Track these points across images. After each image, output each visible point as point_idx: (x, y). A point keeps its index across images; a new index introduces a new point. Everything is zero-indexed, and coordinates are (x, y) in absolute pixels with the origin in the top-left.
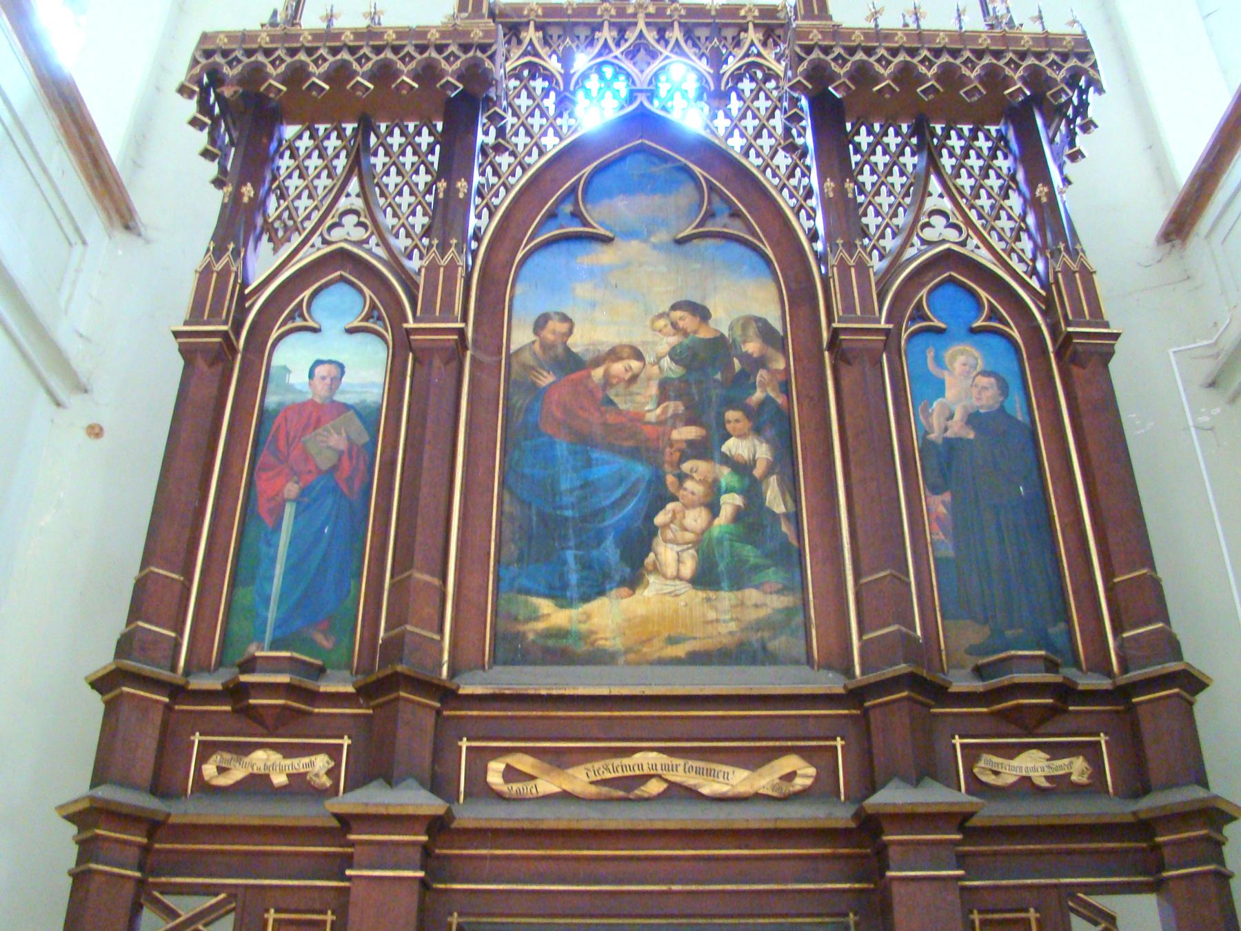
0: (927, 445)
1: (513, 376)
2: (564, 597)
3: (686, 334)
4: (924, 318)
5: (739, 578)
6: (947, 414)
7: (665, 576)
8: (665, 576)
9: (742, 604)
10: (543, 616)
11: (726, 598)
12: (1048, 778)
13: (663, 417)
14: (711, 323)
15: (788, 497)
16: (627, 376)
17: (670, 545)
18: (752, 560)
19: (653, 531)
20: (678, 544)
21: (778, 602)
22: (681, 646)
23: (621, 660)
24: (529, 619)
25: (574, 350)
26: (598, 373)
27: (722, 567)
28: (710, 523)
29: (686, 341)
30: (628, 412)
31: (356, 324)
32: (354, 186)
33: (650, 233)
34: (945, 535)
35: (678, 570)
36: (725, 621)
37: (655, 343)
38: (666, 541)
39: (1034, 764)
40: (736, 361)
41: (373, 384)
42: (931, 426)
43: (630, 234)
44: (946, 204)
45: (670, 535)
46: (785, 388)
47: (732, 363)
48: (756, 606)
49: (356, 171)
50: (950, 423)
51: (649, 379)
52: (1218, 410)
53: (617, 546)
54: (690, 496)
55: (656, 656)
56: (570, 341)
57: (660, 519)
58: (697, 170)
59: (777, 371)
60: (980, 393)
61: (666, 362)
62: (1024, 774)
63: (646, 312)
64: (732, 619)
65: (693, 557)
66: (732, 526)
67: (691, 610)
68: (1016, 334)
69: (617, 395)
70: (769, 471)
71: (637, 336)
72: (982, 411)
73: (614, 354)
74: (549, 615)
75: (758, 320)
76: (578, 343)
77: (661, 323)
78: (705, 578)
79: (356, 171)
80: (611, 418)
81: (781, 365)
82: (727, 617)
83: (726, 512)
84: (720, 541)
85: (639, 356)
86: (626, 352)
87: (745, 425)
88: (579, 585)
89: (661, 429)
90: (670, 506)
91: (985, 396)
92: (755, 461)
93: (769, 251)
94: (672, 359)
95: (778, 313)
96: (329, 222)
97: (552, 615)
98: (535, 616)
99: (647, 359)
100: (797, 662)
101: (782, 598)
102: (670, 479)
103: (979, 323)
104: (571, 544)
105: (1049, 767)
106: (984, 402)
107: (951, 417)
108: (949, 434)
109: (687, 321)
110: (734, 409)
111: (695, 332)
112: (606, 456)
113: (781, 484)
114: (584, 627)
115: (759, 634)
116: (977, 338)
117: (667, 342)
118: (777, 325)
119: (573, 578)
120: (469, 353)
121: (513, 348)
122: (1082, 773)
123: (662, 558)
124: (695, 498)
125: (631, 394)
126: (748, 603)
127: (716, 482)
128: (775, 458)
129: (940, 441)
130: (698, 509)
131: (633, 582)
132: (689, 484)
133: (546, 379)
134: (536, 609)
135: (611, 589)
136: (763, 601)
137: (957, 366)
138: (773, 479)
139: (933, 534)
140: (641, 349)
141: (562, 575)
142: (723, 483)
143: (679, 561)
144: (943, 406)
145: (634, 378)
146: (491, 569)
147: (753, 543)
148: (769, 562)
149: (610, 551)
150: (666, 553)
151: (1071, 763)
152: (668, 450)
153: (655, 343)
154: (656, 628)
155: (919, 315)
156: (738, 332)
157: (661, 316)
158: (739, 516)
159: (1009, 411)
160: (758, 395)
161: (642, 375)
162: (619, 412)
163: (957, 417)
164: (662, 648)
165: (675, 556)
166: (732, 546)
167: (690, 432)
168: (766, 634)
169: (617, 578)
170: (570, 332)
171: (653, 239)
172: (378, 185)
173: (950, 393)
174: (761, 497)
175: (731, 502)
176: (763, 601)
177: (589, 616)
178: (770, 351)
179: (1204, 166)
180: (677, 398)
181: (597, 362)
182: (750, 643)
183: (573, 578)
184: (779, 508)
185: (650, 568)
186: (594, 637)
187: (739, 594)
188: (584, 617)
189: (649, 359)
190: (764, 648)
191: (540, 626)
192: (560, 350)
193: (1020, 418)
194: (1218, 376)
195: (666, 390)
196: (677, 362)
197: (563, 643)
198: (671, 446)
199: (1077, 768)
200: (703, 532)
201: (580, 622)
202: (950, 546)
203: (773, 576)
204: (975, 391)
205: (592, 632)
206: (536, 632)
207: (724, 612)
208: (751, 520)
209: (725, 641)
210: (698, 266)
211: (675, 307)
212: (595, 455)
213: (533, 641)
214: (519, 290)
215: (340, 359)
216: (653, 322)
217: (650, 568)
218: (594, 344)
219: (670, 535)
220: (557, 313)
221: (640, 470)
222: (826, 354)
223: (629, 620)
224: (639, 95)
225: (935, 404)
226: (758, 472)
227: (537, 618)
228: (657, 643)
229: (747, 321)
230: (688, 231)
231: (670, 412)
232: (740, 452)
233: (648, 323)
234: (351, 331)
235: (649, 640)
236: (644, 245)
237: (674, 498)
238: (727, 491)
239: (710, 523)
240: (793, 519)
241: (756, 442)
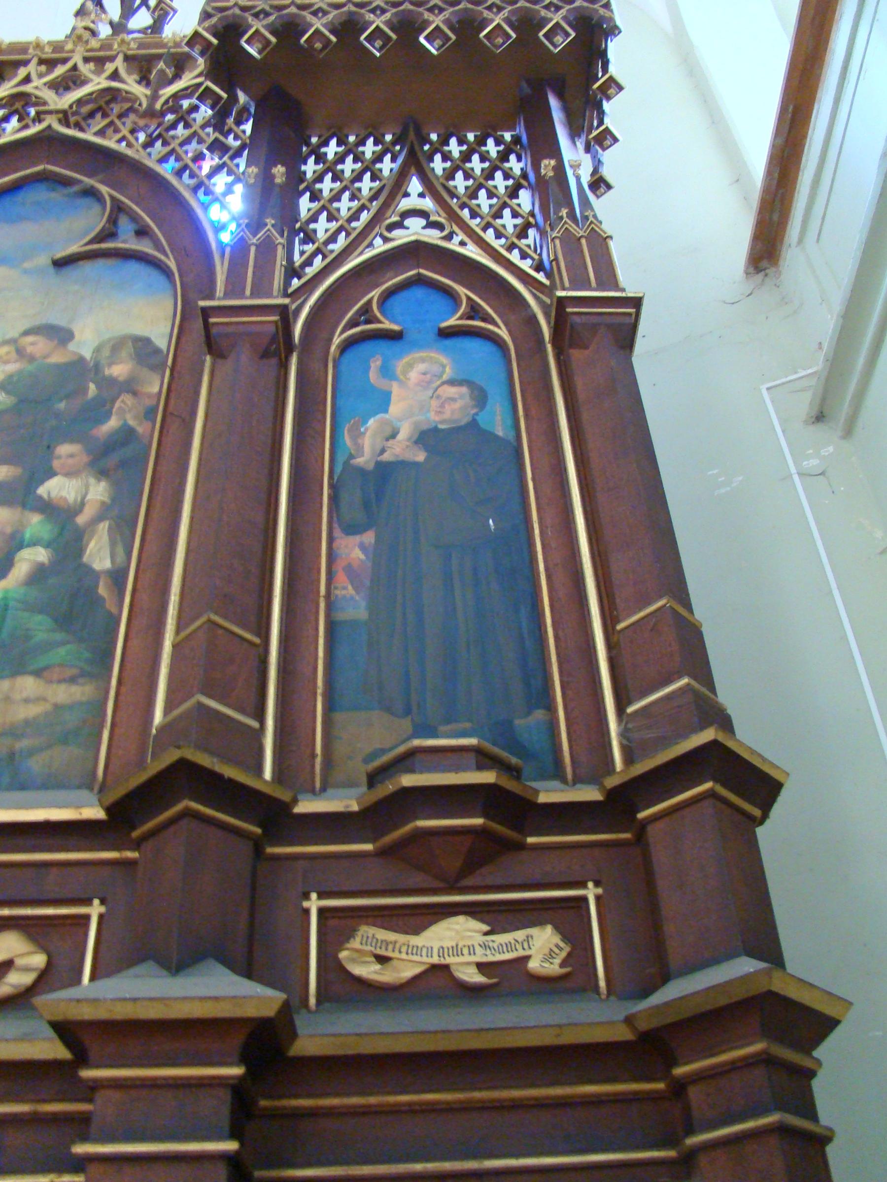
3: (32, 359)
6: (388, 431)
12: (482, 967)
14: (72, 346)
29: (30, 368)
34: (356, 588)
39: (459, 942)
40: (92, 387)
42: (360, 449)
47: (86, 390)
50: (391, 442)
52: (831, 449)
60: (442, 406)
62: (435, 960)
68: (503, 333)
72: (441, 426)
91: (453, 407)
92: (83, 504)
105: (485, 946)
106: (447, 415)
107: (393, 435)
108: (387, 457)
110: (72, 441)
116: (449, 342)
122: (551, 955)
128: (114, 500)
129: (371, 466)
137: (414, 375)
144: (387, 422)
151: (529, 937)
159: (482, 424)
163: (402, 436)
173: (395, 409)
179: (780, 141)
193: (500, 433)
194: (823, 400)
199: (541, 947)
202: (363, 604)
204: (434, 403)
225: (371, 422)
232: (64, 494)
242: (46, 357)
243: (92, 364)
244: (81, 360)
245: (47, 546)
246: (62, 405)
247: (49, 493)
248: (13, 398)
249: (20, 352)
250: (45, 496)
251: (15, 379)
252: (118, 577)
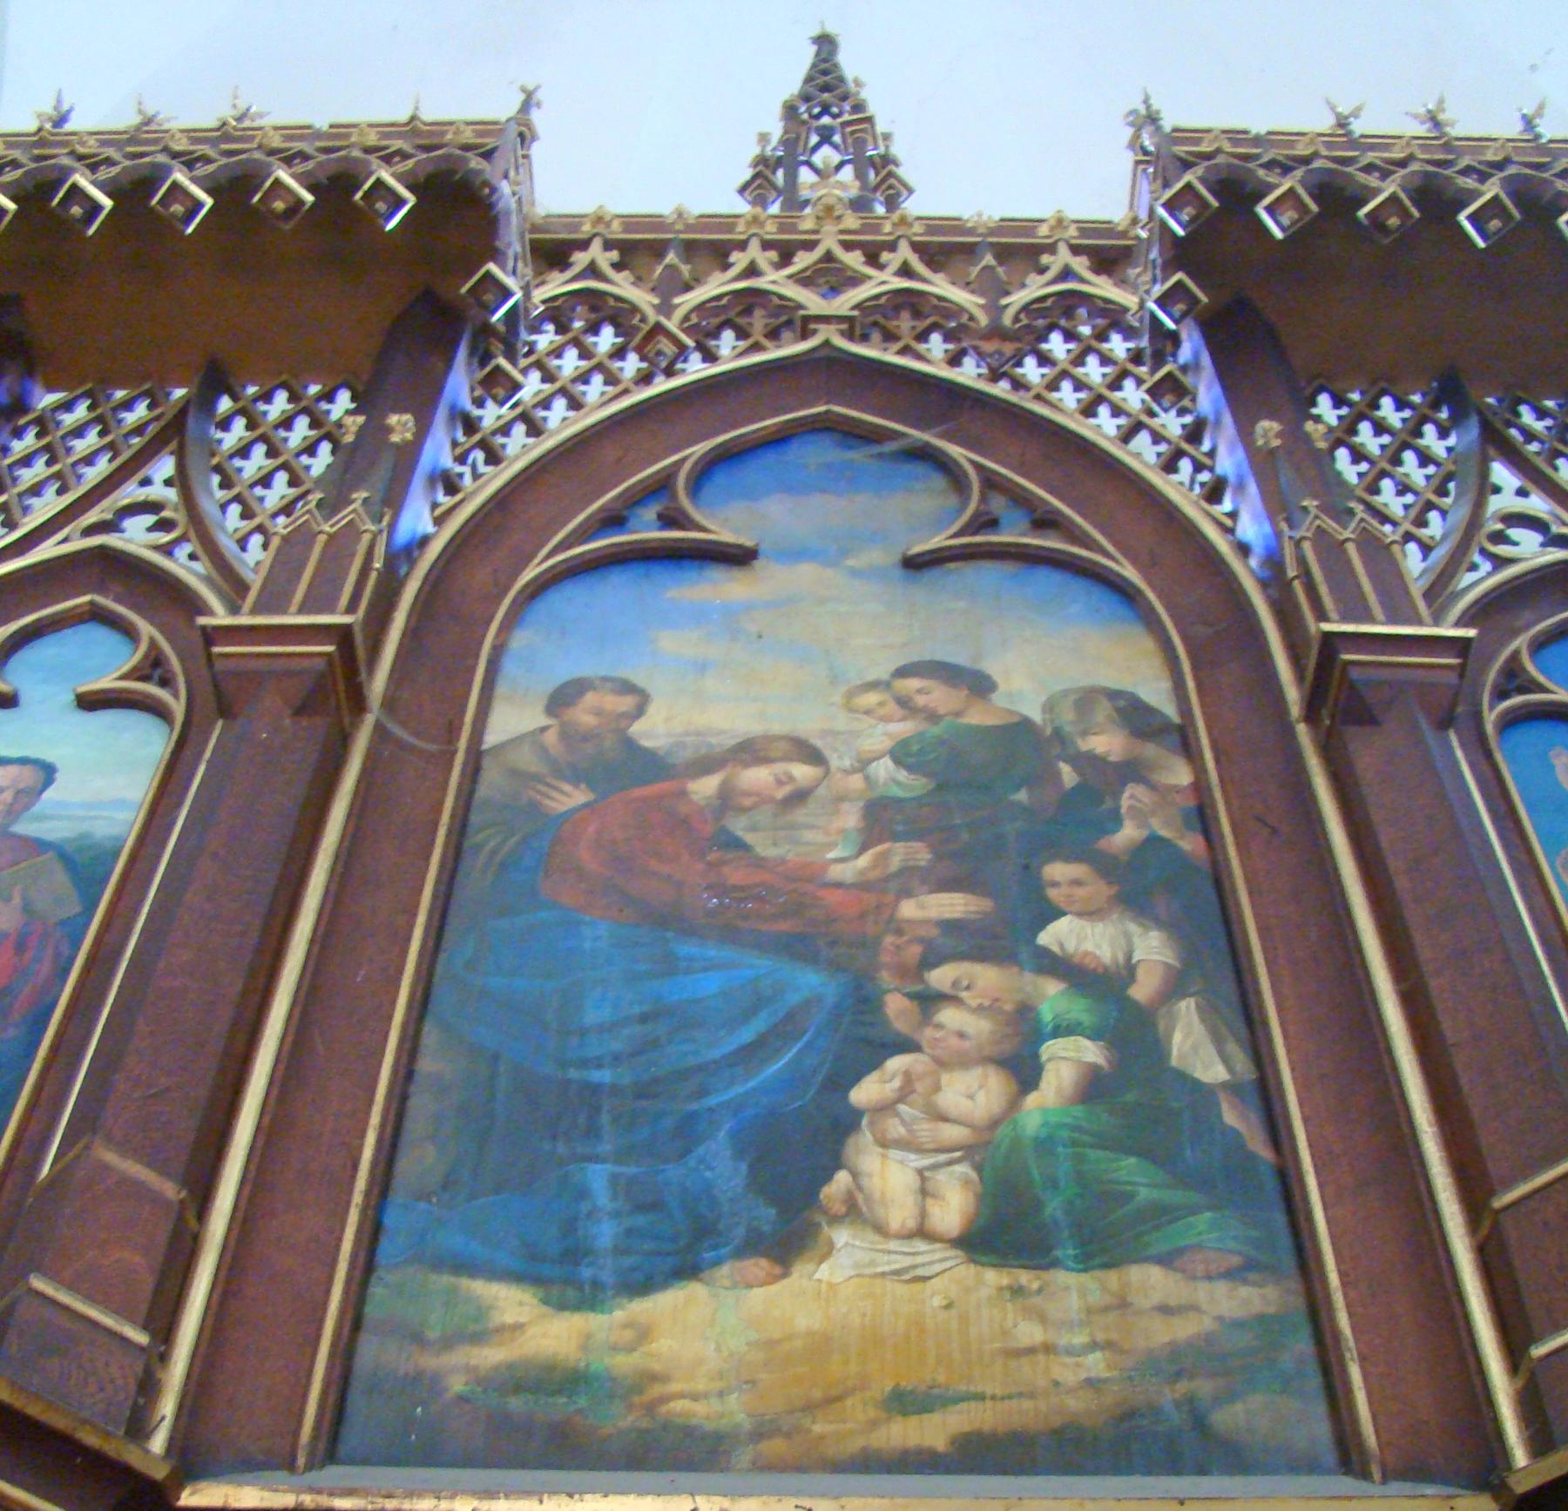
1: (482, 791)
2: (572, 1281)
3: (933, 717)
5: (1105, 1239)
7: (880, 1229)
8: (880, 1229)
9: (1123, 1304)
10: (501, 1330)
11: (1072, 1290)
13: (874, 875)
14: (998, 699)
15: (1232, 1048)
16: (781, 793)
17: (894, 1154)
18: (1144, 1194)
19: (846, 1122)
20: (920, 1150)
21: (1229, 1302)
22: (936, 1417)
23: (744, 1456)
24: (449, 1342)
25: (646, 743)
26: (705, 787)
27: (1053, 1207)
28: (1014, 1104)
29: (935, 730)
30: (783, 861)
31: (106, 683)
32: (165, 467)
33: (844, 553)
35: (923, 1214)
36: (1070, 1351)
37: (855, 734)
38: (884, 1143)
40: (1065, 769)
41: (118, 804)
43: (795, 554)
44: (1537, 504)
46: (1203, 819)
48: (1165, 1310)
49: (174, 445)
51: (841, 799)
53: (739, 1154)
54: (954, 1042)
55: (855, 1445)
56: (637, 728)
57: (865, 1092)
58: (955, 451)
59: (1177, 789)
61: (884, 769)
63: (834, 681)
64: (1094, 1346)
65: (967, 1182)
66: (1079, 1111)
67: (964, 1319)
69: (753, 829)
70: (1175, 987)
71: (808, 723)
73: (750, 751)
74: (518, 1327)
75: (1113, 695)
76: (655, 729)
77: (871, 699)
78: (1006, 1231)
79: (174, 445)
80: (735, 875)
81: (1182, 775)
82: (1080, 1339)
84: (1044, 1145)
85: (813, 756)
86: (783, 746)
87: (1099, 890)
88: (619, 1251)
89: (870, 899)
90: (896, 1063)
93: (1129, 572)
94: (898, 762)
95: (1166, 685)
96: (91, 517)
97: (530, 1327)
99: (835, 762)
100: (1310, 1466)
101: (1244, 1291)
102: (896, 1007)
104: (605, 1148)
109: (938, 696)
110: (1069, 859)
111: (958, 714)
112: (712, 952)
113: (1207, 1012)
114: (623, 1363)
115: (1183, 1387)
117: (880, 735)
118: (1156, 693)
119: (605, 1233)
120: (370, 720)
121: (491, 739)
123: (874, 1184)
124: (967, 1044)
125: (793, 827)
126: (1142, 1302)
130: (977, 1072)
131: (788, 1239)
132: (949, 1016)
134: (482, 1311)
135: (717, 1262)
138: (1187, 1008)
140: (818, 743)
141: (570, 1227)
142: (1047, 1013)
143: (924, 1192)
145: (800, 797)
146: (358, 1198)
147: (1147, 1154)
148: (1192, 1197)
149: (720, 1167)
150: (884, 1173)
152: (889, 940)
153: (855, 734)
154: (853, 1368)
155: (1514, 679)
156: (1067, 717)
157: (874, 685)
158: (1093, 1087)
160: (1128, 834)
161: (821, 791)
162: (761, 863)
164: (873, 1424)
165: (912, 1180)
166: (1080, 1159)
167: (954, 905)
168: (1204, 1388)
169: (740, 1231)
170: (640, 711)
171: (850, 562)
172: (218, 469)
174: (1157, 1049)
175: (1068, 1060)
176: (1190, 1299)
177: (643, 1333)
178: (1150, 750)
180: (906, 836)
181: (705, 765)
182: (1155, 1411)
183: (605, 1233)
184: (1212, 1072)
185: (839, 1208)
186: (656, 1390)
187: (1112, 1278)
188: (629, 1334)
189: (839, 760)
190: (1199, 1422)
191: (491, 1356)
192: (609, 742)
195: (881, 820)
196: (910, 769)
197: (560, 1406)
198: (899, 932)
200: (994, 1124)
201: (614, 1348)
205: (654, 1378)
206: (470, 1370)
207: (1070, 1326)
208: (1130, 1097)
209: (1076, 1404)
210: (962, 604)
211: (902, 672)
212: (687, 949)
213: (462, 1399)
214: (520, 640)
215: (48, 755)
216: (851, 694)
217: (839, 1208)
218: (698, 734)
219: (895, 1129)
220: (605, 679)
221: (810, 983)
222: (1302, 730)
223: (771, 1344)
224: (821, 327)
226: (1143, 990)
227: (478, 1338)
228: (858, 1410)
229: (1087, 699)
230: (938, 541)
231: (895, 863)
232: (1089, 946)
233: (838, 698)
234: (90, 702)
235: (830, 1401)
236: (829, 572)
237: (907, 1045)
238: (1059, 1031)
239: (1014, 1104)
240: (1255, 1100)
241: (1133, 928)
242: (958, 714)
243: (1048, 731)
244: (1025, 724)
245: (1095, 1035)
246: (1022, 796)
247: (1061, 946)
248: (924, 780)
249: (904, 702)
250: (1055, 949)
251: (915, 748)
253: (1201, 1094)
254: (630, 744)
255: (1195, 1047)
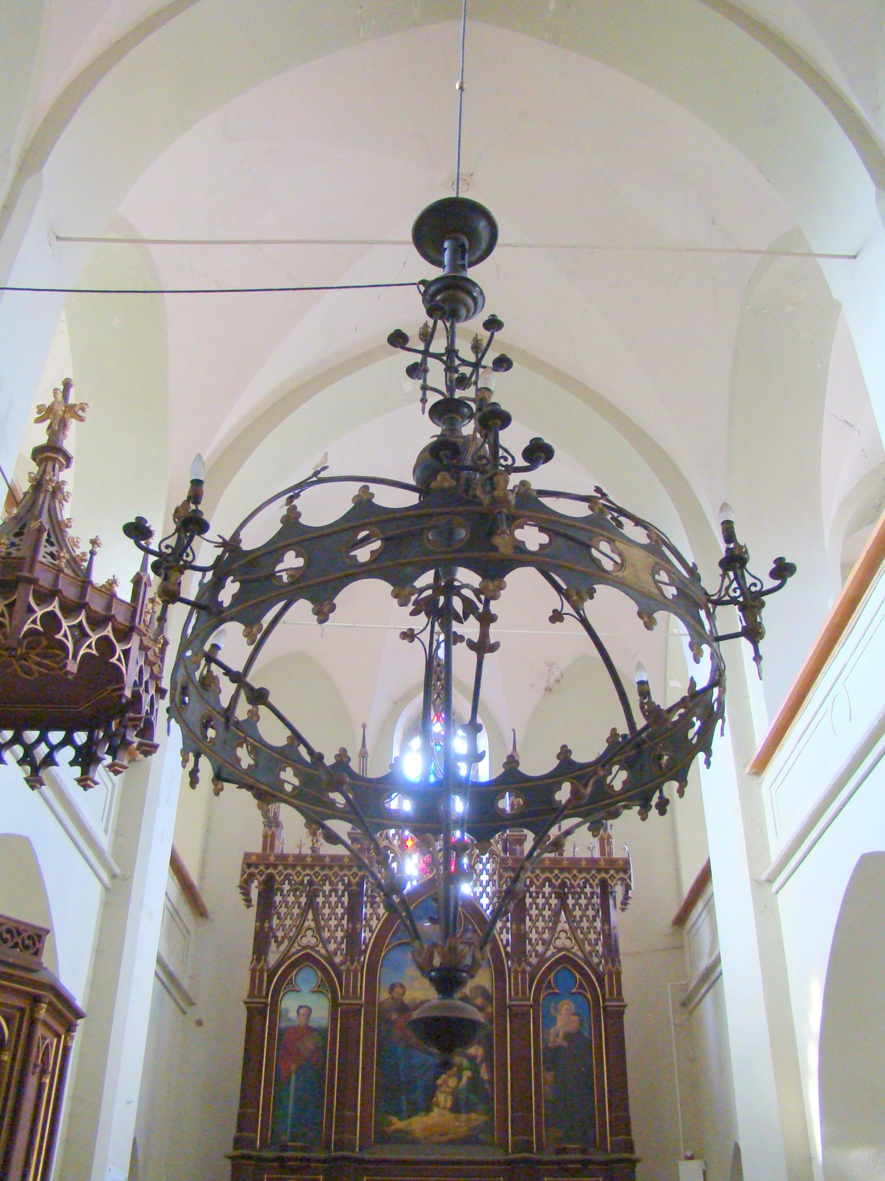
0: (546, 1048)
4: (551, 988)
5: (470, 1108)
9: (469, 1119)
11: (464, 1117)
27: (462, 1103)
28: (458, 1083)
45: (442, 1089)
57: (439, 1082)
70: (482, 1062)
83: (465, 1079)
98: (390, 1124)
103: (574, 990)
119: (404, 1108)
127: (461, 1064)
133: (394, 1016)
136: (477, 1118)
138: (484, 1065)
139: (545, 1090)
143: (446, 1100)
149: (418, 1096)
174: (479, 1073)
175: (467, 1074)
176: (477, 1118)
203: (482, 1107)
226: (478, 1060)
239: (458, 1083)
252: (491, 1081)
253: (483, 1081)
254: (403, 1004)
255: (484, 1074)
